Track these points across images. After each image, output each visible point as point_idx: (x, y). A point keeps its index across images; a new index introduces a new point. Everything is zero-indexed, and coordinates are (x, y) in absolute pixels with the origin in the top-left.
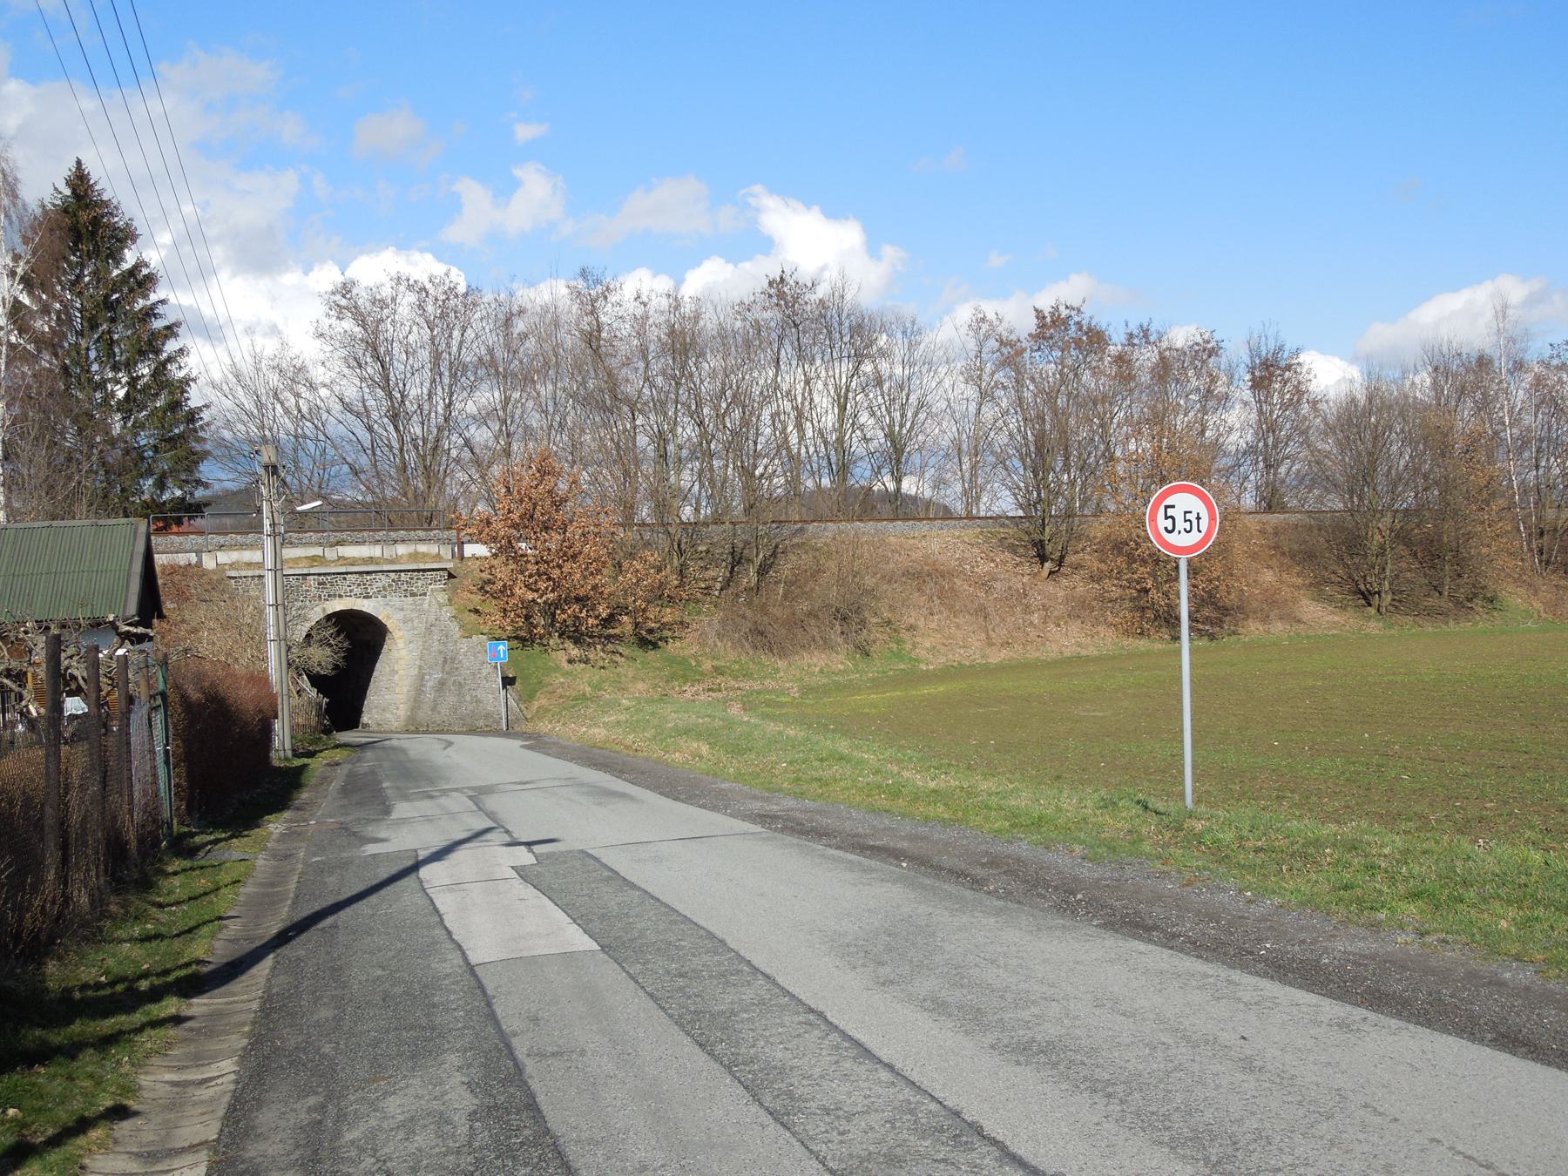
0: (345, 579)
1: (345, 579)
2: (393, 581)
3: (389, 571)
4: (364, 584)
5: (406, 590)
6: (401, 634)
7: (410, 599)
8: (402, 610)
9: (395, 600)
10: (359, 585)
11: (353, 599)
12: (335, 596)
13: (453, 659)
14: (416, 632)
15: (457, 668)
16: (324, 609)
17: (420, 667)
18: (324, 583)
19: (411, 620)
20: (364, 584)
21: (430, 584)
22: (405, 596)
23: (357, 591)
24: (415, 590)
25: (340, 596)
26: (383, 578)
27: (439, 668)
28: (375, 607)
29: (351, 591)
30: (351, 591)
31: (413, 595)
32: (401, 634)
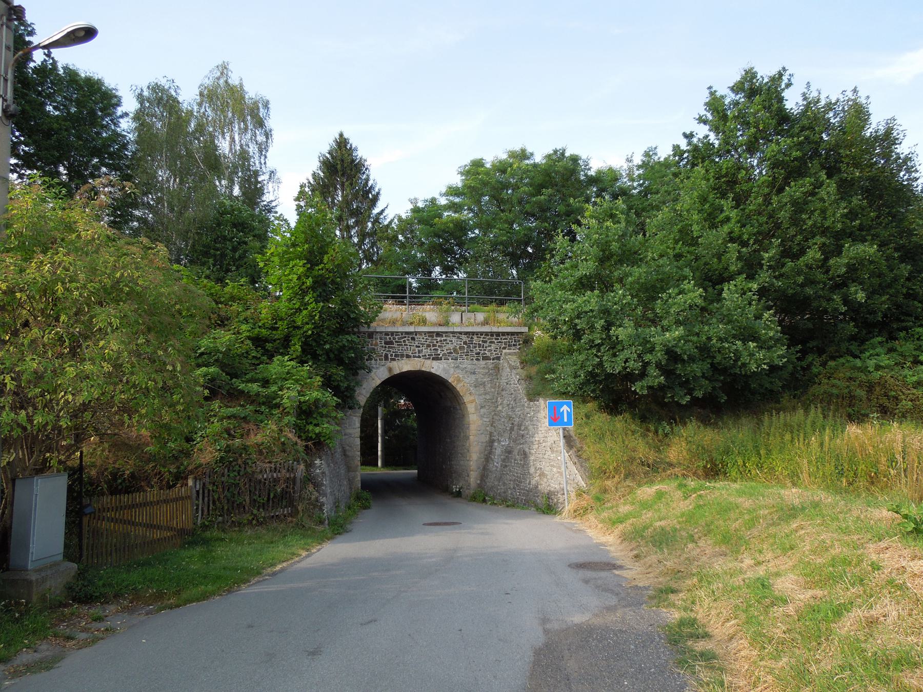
0: (413, 339)
1: (413, 339)
2: (465, 343)
3: (460, 333)
4: (434, 346)
5: (478, 354)
6: (472, 398)
7: (482, 363)
8: (474, 373)
9: (467, 364)
10: (428, 346)
11: (421, 359)
12: (402, 356)
13: (520, 426)
14: (488, 397)
15: (523, 436)
16: (390, 370)
17: (491, 434)
18: (391, 343)
19: (484, 384)
20: (434, 346)
21: (504, 348)
22: (477, 360)
23: (426, 351)
24: (488, 354)
25: (408, 356)
26: (454, 339)
27: (507, 435)
28: (444, 369)
29: (419, 352)
30: (419, 352)
31: (486, 358)
32: (472, 398)
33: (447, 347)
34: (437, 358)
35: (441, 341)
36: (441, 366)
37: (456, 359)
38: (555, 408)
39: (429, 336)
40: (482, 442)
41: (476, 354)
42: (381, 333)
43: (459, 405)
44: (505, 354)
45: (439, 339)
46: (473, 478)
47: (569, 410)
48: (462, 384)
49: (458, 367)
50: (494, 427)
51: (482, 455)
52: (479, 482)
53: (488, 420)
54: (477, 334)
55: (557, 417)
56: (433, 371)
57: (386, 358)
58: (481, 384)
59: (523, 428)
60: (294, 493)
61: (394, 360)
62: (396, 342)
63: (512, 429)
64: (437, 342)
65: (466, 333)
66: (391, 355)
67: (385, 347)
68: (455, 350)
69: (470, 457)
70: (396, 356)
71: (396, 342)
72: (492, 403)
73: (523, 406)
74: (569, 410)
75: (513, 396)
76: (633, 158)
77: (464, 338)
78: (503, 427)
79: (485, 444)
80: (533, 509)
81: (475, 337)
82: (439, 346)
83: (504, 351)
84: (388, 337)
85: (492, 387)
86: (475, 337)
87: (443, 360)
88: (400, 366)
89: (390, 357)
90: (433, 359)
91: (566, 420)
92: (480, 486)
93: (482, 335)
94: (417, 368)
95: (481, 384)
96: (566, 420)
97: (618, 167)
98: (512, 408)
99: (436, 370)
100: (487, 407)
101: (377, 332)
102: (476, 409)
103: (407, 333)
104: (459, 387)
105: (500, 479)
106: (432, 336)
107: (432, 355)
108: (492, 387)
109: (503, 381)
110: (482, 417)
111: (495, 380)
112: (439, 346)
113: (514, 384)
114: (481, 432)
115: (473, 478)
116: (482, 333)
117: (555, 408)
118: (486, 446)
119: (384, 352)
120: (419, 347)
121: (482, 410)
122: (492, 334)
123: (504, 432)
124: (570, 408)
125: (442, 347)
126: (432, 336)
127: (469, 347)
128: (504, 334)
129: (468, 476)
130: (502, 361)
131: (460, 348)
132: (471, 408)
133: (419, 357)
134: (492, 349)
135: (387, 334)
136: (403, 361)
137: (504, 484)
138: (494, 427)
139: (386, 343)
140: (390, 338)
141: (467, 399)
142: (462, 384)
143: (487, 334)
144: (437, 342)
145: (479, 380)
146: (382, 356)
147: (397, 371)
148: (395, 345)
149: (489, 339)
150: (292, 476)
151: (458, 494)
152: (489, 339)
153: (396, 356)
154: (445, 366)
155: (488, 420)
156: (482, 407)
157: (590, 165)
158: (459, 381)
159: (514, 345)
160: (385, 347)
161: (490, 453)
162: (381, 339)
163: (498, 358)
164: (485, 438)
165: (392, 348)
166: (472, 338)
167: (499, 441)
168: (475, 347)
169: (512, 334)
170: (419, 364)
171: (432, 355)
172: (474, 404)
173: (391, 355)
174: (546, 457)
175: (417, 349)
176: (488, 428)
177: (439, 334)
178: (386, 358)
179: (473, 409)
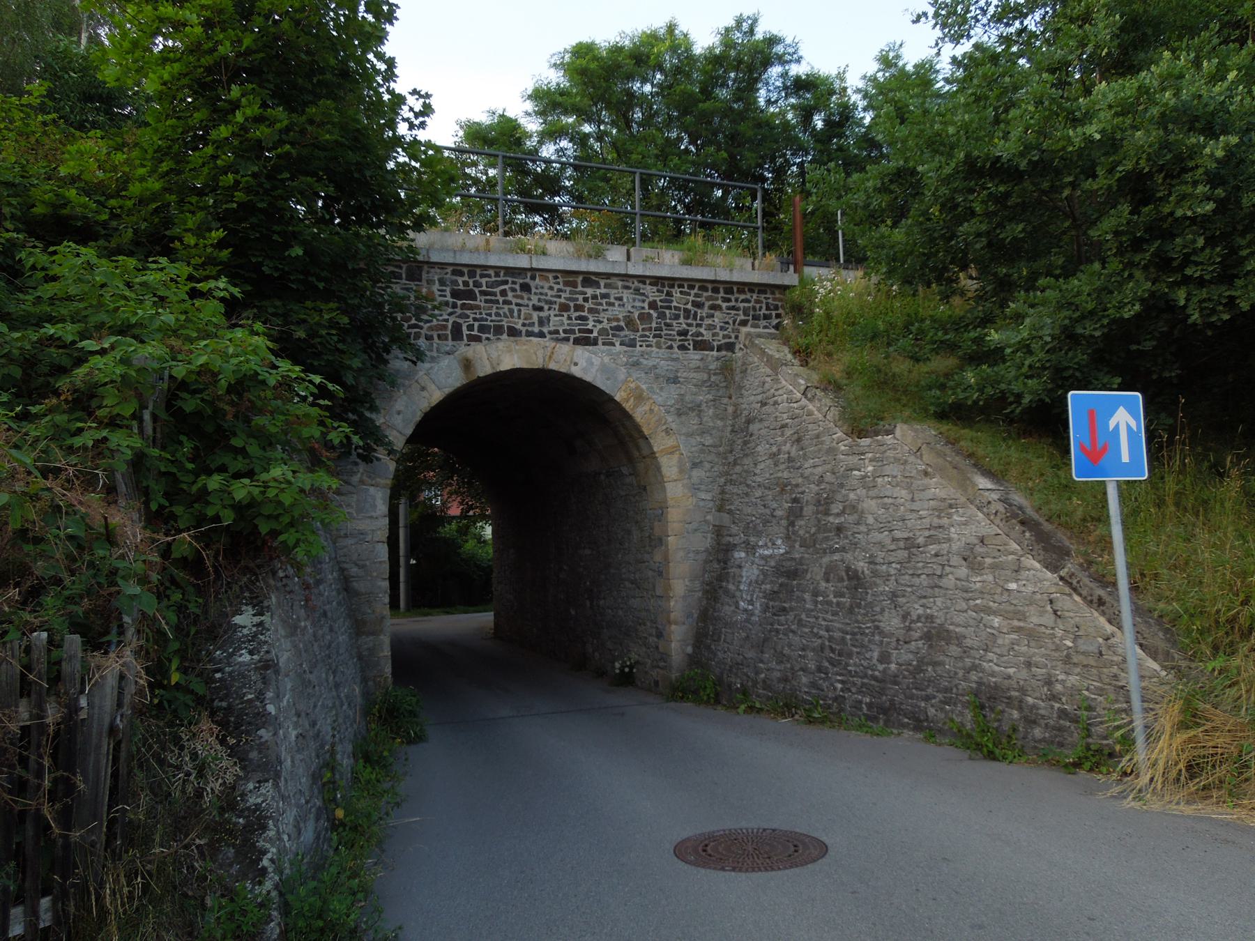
0: (526, 288)
1: (526, 288)
2: (653, 305)
3: (642, 279)
4: (578, 308)
5: (683, 333)
6: (670, 442)
7: (694, 356)
8: (675, 380)
9: (657, 357)
10: (564, 308)
11: (547, 342)
12: (498, 330)
13: (824, 505)
14: (708, 441)
15: (839, 529)
16: (467, 365)
17: (719, 531)
18: (470, 295)
19: (697, 408)
20: (578, 308)
21: (744, 323)
22: (682, 348)
23: (559, 322)
24: (707, 336)
25: (513, 332)
26: (626, 295)
27: (778, 530)
28: (604, 369)
29: (541, 322)
30: (541, 322)
31: (701, 345)
32: (670, 442)
33: (609, 314)
34: (585, 340)
35: (595, 297)
36: (596, 361)
37: (632, 344)
38: (1092, 414)
39: (566, 284)
40: (697, 552)
41: (681, 333)
42: (442, 266)
43: (631, 460)
44: (748, 334)
45: (590, 292)
46: (678, 641)
47: (1133, 424)
48: (647, 408)
49: (636, 364)
50: (730, 512)
51: (697, 584)
52: (689, 650)
53: (708, 496)
54: (681, 286)
55: (1100, 445)
56: (576, 371)
57: (457, 333)
58: (692, 409)
59: (836, 508)
60: (66, 819)
61: (477, 339)
62: (483, 293)
63: (795, 513)
64: (586, 300)
65: (657, 281)
66: (470, 328)
67: (455, 306)
68: (630, 322)
69: (668, 587)
70: (483, 329)
71: (483, 293)
72: (719, 454)
73: (832, 451)
74: (1134, 427)
75: (788, 432)
76: (847, 75)
77: (650, 291)
78: (762, 510)
79: (704, 556)
80: (907, 733)
81: (676, 292)
82: (591, 310)
83: (744, 330)
84: (460, 280)
85: (716, 416)
86: (676, 292)
87: (600, 346)
88: (494, 355)
89: (465, 332)
90: (577, 342)
91: (1125, 458)
92: (694, 660)
93: (691, 287)
94: (537, 362)
95: (692, 409)
96: (1125, 458)
97: (834, 73)
98: (790, 460)
99: (584, 370)
100: (707, 465)
101: (433, 265)
102: (681, 471)
103: (512, 271)
104: (640, 414)
105: (761, 646)
106: (574, 285)
107: (572, 332)
108: (716, 416)
109: (750, 401)
110: (695, 488)
111: (725, 400)
112: (591, 310)
113: (790, 401)
114: (694, 525)
115: (678, 641)
116: (691, 283)
117: (1092, 414)
118: (706, 562)
119: (452, 319)
120: (540, 309)
121: (696, 473)
122: (715, 285)
123: (766, 522)
124: (1136, 418)
125: (597, 311)
126: (574, 285)
127: (662, 316)
128: (744, 287)
129: (660, 635)
130: (739, 354)
131: (641, 317)
132: (669, 467)
133: (541, 335)
134: (714, 325)
135: (458, 269)
136: (501, 345)
137: (781, 658)
138: (730, 512)
139: (455, 294)
140: (466, 284)
141: (660, 443)
142: (647, 408)
143: (703, 284)
144: (586, 300)
145: (688, 398)
146: (445, 327)
147: (484, 369)
148: (480, 301)
149: (708, 299)
150: (52, 714)
151: (626, 680)
152: (708, 299)
153: (483, 329)
154: (606, 360)
155: (708, 496)
156: (695, 465)
157: (801, 53)
158: (640, 398)
159: (766, 317)
160: (455, 306)
161: (722, 577)
162: (442, 282)
163: (730, 347)
164: (704, 542)
165: (471, 308)
166: (669, 294)
167: (751, 549)
168: (677, 317)
169: (762, 288)
170: (540, 353)
171: (572, 332)
172: (676, 457)
173: (470, 328)
174: (949, 581)
175: (535, 315)
176: (709, 517)
177: (589, 279)
178: (457, 333)
179: (675, 470)
